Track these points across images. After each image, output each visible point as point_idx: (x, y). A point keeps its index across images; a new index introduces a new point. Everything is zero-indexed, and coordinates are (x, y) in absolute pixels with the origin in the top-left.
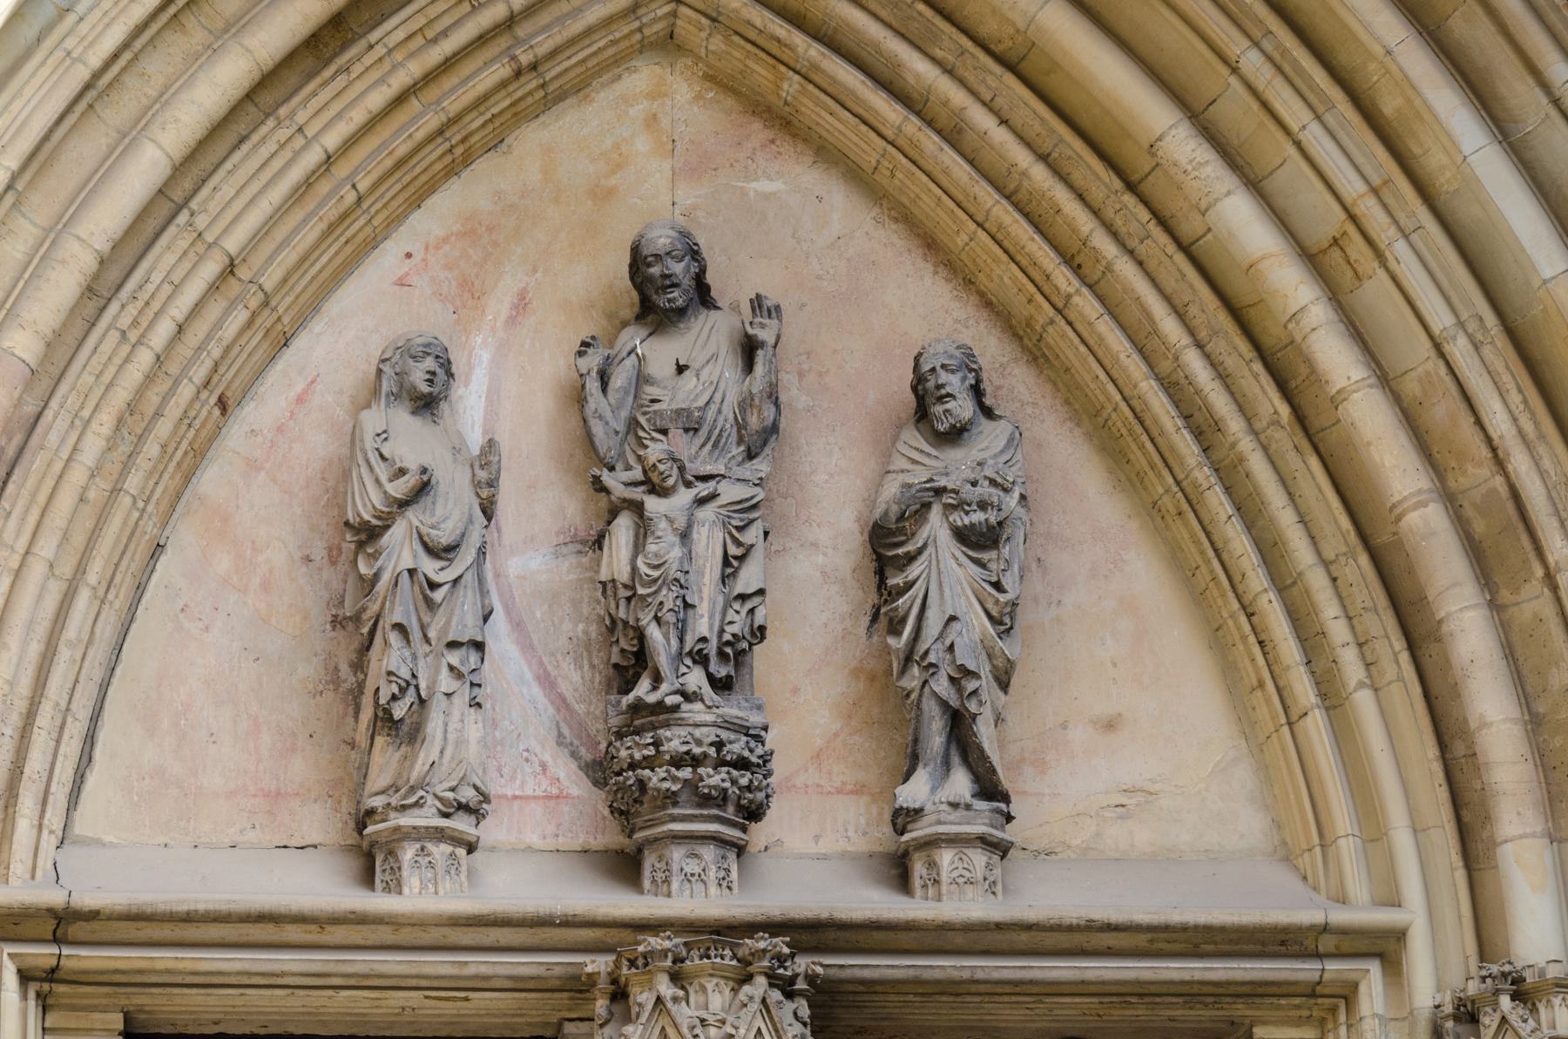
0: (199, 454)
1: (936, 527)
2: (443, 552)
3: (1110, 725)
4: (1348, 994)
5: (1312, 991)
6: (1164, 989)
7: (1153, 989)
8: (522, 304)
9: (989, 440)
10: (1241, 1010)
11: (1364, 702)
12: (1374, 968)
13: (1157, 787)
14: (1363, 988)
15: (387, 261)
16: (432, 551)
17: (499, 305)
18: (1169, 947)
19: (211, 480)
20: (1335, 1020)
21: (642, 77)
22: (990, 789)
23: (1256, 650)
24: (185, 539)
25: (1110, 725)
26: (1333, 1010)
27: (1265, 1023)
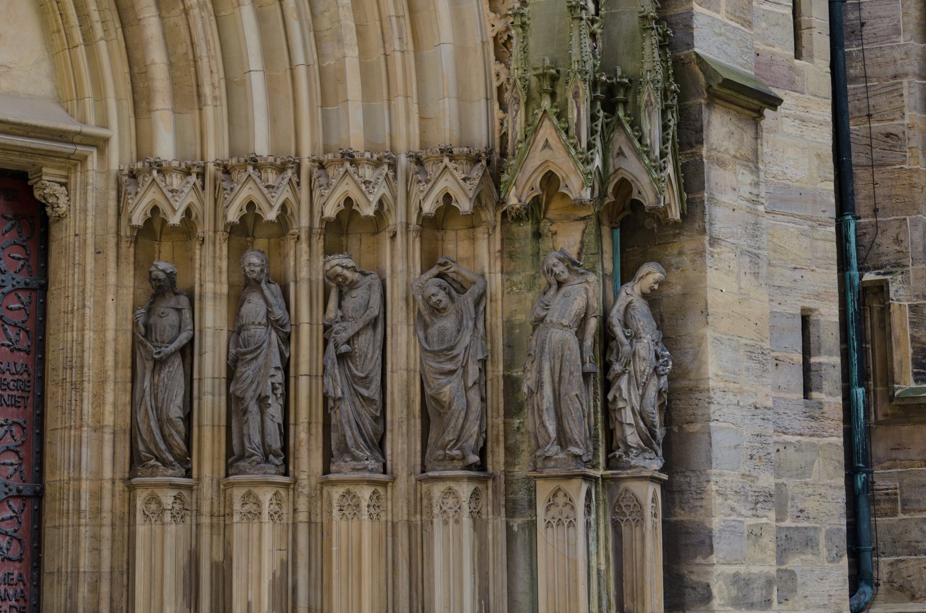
4: (83, 159)
5: (68, 157)
6: (12, 148)
7: (8, 148)
10: (39, 161)
11: (102, 45)
12: (95, 151)
13: (12, 66)
14: (89, 159)
18: (17, 132)
20: (75, 170)
23: (59, 17)
26: (75, 165)
27: (47, 167)
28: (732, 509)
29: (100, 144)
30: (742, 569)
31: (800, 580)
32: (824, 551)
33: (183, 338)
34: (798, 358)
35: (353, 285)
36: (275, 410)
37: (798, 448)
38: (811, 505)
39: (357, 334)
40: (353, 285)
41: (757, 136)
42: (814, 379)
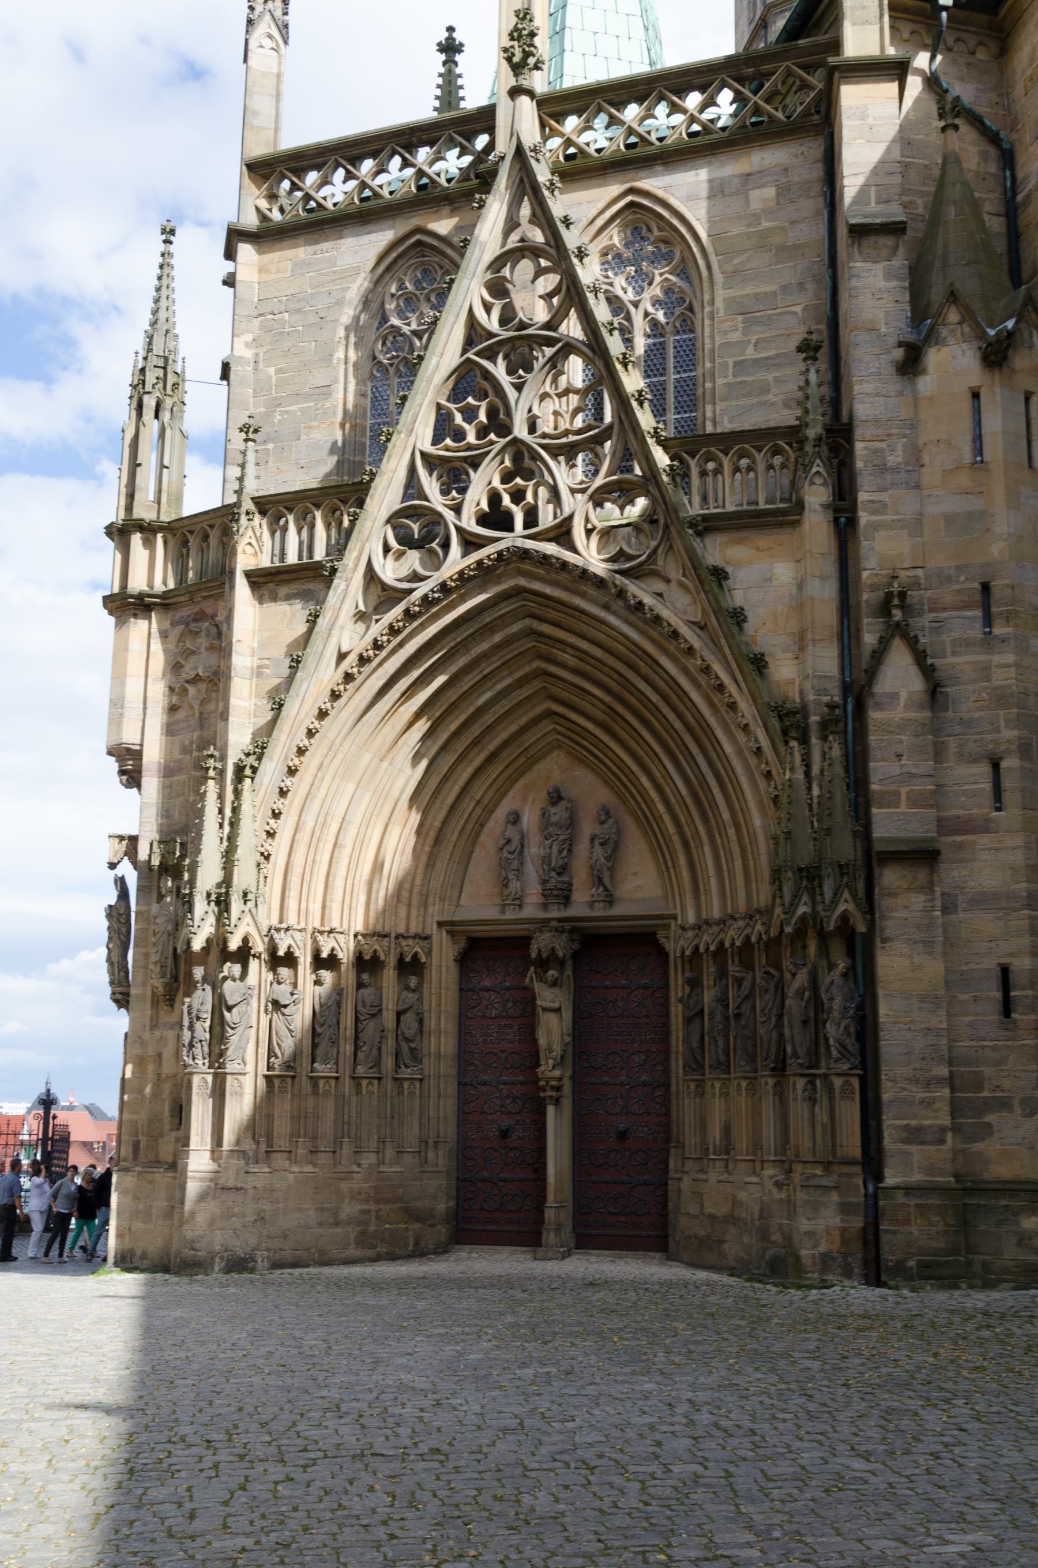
0: (477, 835)
1: (597, 842)
2: (512, 853)
3: (635, 874)
4: (669, 926)
5: (664, 925)
8: (534, 800)
9: (610, 822)
15: (511, 794)
16: (512, 853)
17: (530, 801)
19: (482, 838)
21: (556, 753)
22: (606, 889)
24: (477, 849)
25: (635, 874)
28: (904, 1089)
29: (674, 917)
30: (914, 1122)
31: (995, 1128)
32: (1018, 1110)
33: (697, 1009)
34: (998, 995)
35: (743, 979)
36: (721, 1043)
37: (994, 1049)
38: (1006, 1083)
39: (741, 1004)
40: (743, 979)
41: (932, 872)
42: (1012, 1006)
